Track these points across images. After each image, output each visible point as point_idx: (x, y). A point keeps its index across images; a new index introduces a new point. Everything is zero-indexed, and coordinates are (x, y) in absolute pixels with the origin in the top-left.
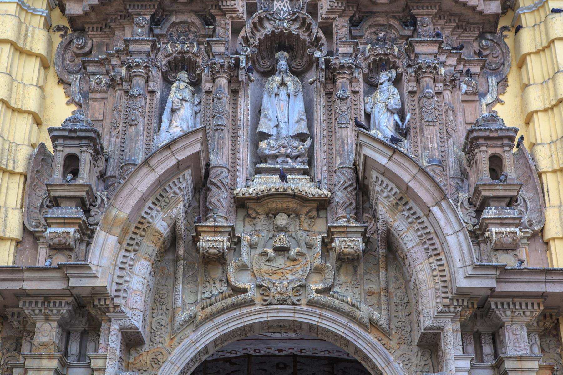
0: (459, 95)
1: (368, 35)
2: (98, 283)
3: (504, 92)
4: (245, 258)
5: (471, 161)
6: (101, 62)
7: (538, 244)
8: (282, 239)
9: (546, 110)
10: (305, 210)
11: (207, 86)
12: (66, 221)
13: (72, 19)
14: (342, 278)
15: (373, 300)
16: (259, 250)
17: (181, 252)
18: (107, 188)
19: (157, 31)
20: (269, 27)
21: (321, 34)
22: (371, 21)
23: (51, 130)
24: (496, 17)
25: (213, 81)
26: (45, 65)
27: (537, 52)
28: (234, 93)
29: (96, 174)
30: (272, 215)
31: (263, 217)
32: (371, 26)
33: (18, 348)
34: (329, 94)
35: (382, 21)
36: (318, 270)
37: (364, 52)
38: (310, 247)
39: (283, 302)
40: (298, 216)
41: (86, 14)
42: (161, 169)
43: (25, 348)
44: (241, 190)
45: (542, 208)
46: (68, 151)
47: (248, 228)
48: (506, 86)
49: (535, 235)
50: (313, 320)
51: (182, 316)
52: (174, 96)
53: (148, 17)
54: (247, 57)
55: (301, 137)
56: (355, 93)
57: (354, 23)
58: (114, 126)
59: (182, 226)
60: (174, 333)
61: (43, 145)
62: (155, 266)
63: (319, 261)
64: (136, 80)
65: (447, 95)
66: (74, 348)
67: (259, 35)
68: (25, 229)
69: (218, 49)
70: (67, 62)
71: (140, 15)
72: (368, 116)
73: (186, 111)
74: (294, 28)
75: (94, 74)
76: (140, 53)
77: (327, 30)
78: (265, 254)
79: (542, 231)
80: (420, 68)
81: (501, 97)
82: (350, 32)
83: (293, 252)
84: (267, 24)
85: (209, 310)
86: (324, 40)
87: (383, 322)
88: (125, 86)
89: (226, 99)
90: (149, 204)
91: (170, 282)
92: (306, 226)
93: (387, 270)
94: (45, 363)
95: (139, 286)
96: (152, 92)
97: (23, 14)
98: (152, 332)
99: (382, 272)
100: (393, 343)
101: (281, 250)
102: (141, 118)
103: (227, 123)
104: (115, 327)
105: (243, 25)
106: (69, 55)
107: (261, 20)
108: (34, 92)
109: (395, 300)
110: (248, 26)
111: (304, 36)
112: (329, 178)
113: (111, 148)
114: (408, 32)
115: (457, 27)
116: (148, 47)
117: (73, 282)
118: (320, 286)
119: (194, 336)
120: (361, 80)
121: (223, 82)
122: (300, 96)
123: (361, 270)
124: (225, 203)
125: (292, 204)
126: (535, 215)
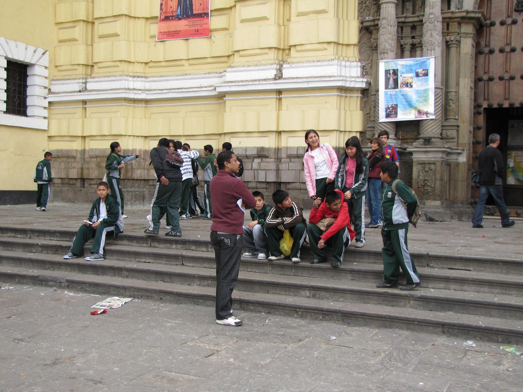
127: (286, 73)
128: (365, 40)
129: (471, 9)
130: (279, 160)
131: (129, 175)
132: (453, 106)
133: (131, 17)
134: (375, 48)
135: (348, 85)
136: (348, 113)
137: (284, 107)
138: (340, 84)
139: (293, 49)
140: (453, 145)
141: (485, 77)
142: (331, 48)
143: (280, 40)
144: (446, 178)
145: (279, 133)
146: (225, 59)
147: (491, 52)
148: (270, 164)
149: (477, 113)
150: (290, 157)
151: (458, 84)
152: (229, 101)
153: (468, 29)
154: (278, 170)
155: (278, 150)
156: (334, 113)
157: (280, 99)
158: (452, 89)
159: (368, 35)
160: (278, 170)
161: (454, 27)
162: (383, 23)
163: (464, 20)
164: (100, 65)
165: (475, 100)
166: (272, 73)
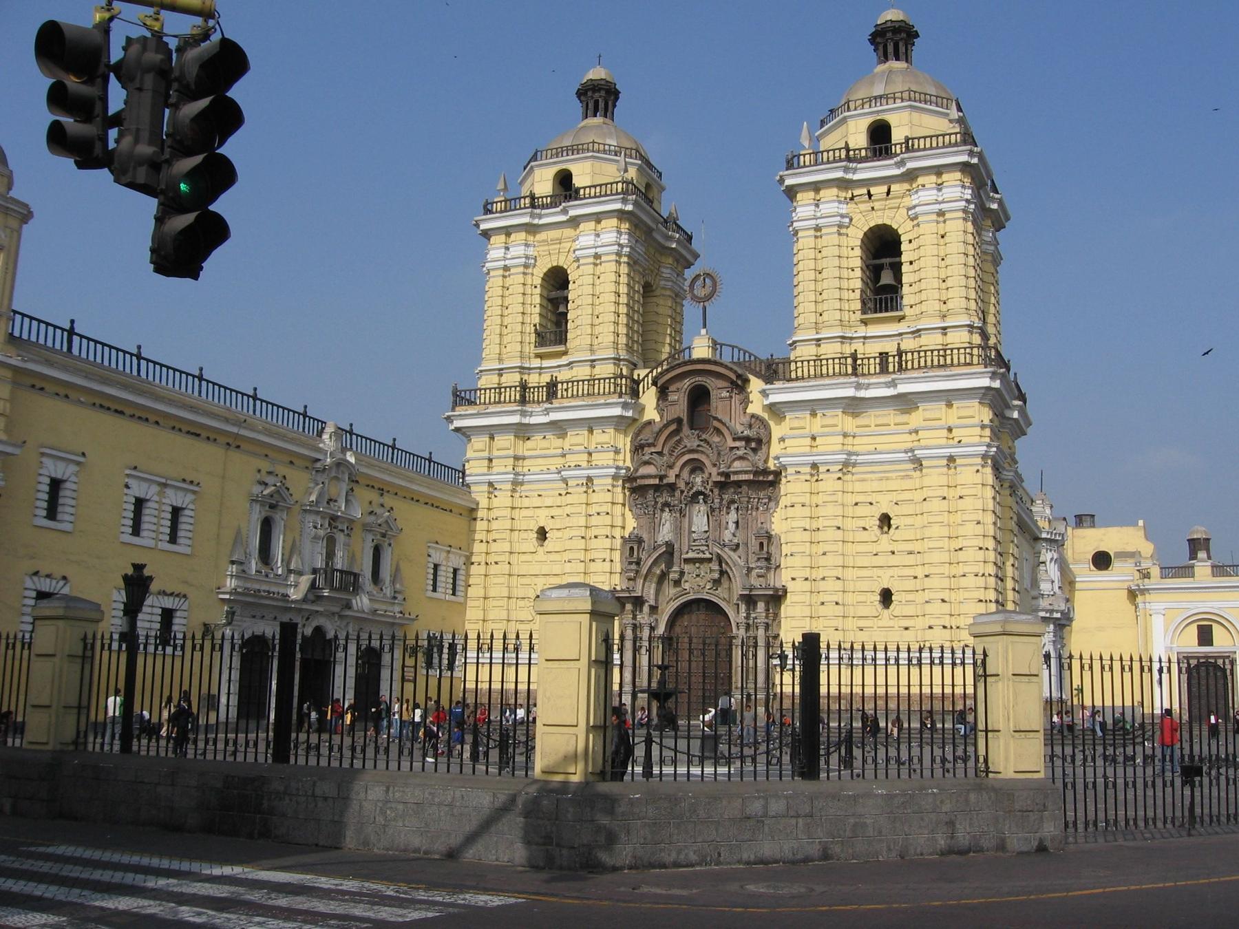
2: (640, 595)
7: (778, 570)
12: (632, 570)
20: (695, 489)
26: (624, 505)
42: (654, 557)
50: (708, 598)
52: (663, 521)
54: (686, 505)
55: (706, 532)
67: (691, 493)
68: (622, 569)
73: (668, 525)
77: (712, 491)
79: (780, 566)
101: (698, 576)
104: (647, 604)
106: (631, 499)
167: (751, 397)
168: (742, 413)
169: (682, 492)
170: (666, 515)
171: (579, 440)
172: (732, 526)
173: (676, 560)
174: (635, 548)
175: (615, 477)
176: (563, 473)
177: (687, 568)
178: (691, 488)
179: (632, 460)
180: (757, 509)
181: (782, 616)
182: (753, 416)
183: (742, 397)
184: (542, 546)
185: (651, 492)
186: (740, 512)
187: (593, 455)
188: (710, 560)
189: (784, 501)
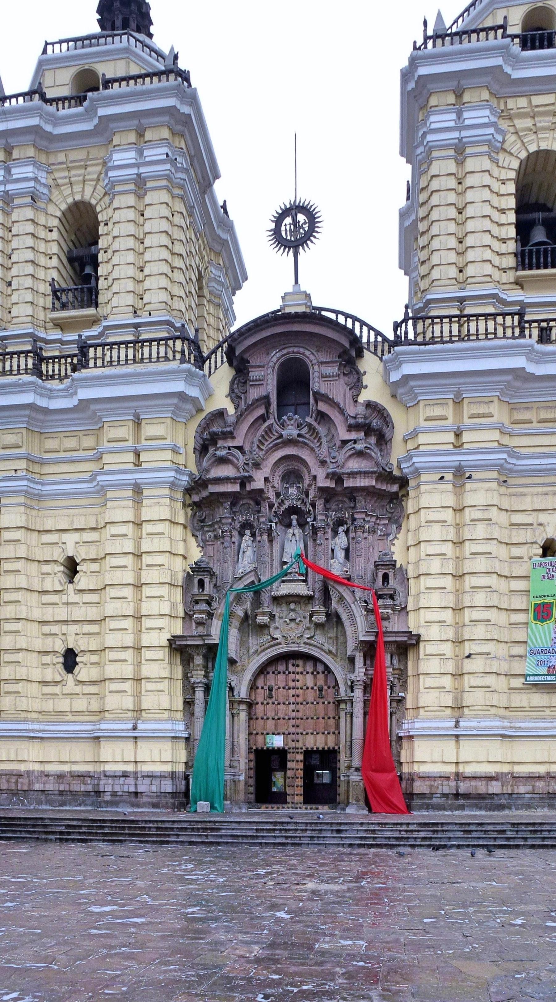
0: (376, 537)
1: (334, 507)
3: (399, 533)
4: (277, 624)
5: (377, 574)
6: (210, 526)
7: (403, 613)
8: (292, 615)
9: (414, 545)
10: (302, 601)
11: (258, 538)
12: (201, 612)
13: (195, 503)
14: (318, 632)
15: (331, 641)
16: (283, 620)
17: (250, 622)
18: (218, 591)
19: (234, 510)
20: (287, 504)
21: (311, 508)
22: (336, 499)
23: (191, 568)
24: (396, 493)
25: (261, 536)
27: (414, 513)
28: (271, 541)
29: (212, 585)
30: (288, 603)
31: (284, 605)
32: (335, 502)
33: (189, 664)
34: (315, 540)
35: (341, 498)
36: (308, 628)
37: (331, 517)
38: (305, 618)
39: (294, 643)
40: (300, 603)
41: (201, 501)
43: (191, 665)
44: (275, 593)
45: (408, 594)
46: (199, 577)
47: (279, 609)
48: (401, 529)
49: (403, 609)
51: (251, 651)
52: (243, 545)
53: (229, 503)
54: (276, 523)
56: (327, 539)
57: (327, 501)
58: (218, 560)
59: (249, 612)
60: (249, 657)
61: (188, 572)
62: (239, 630)
63: (308, 625)
64: (226, 538)
65: (370, 538)
66: (210, 665)
67: (282, 509)
68: (186, 613)
69: (262, 520)
70: (195, 524)
71: (225, 502)
72: (333, 550)
73: (249, 552)
74: (299, 504)
75: (208, 531)
76: (226, 524)
78: (286, 622)
80: (356, 527)
81: (397, 536)
82: (325, 506)
83: (297, 621)
84: (286, 502)
85: (263, 647)
86: (312, 512)
87: (334, 651)
88: (222, 540)
89: (267, 544)
90: (234, 604)
91: (246, 635)
92: (303, 608)
93: (337, 628)
94: (199, 672)
95: (233, 640)
96: (234, 543)
97: (173, 502)
98: (241, 657)
99: (335, 629)
100: (338, 660)
102: (229, 559)
103: (267, 559)
105: (274, 505)
107: (282, 501)
108: (182, 544)
109: (340, 641)
110: (276, 506)
111: (303, 508)
112: (314, 585)
113: (218, 572)
114: (352, 505)
115: (378, 498)
116: (230, 520)
117: (206, 642)
118: (308, 636)
119: (257, 658)
120: (330, 530)
121: (265, 537)
122: (302, 541)
123: (326, 629)
124: (267, 599)
125: (296, 599)
126: (404, 599)
127: (140, 726)
128: (186, 708)
129: (244, 697)
130: (136, 778)
131: (31, 787)
132: (236, 749)
133: (28, 681)
134: (193, 714)
135: (177, 735)
136: (178, 752)
137: (139, 747)
138: (173, 735)
139: (143, 712)
140: (236, 771)
141: (254, 732)
142: (166, 715)
143: (134, 705)
144: (233, 788)
145: (136, 762)
146: (98, 714)
147: (257, 719)
148: (131, 781)
149: (250, 752)
150: (143, 777)
151: (239, 737)
152: (103, 742)
153: (243, 707)
154: (136, 785)
155: (135, 773)
156: (169, 752)
157: (136, 742)
158: (236, 740)
159: (188, 706)
160: (136, 785)
161: (236, 706)
162: (197, 702)
163: (240, 702)
164: (6, 712)
165: (249, 745)
166: (130, 726)
167: (366, 380)
168: (352, 402)
169: (271, 506)
170: (247, 538)
171: (121, 432)
172: (340, 554)
173: (265, 597)
174: (207, 580)
175: (173, 486)
176: (99, 478)
177: (277, 611)
178: (282, 501)
179: (199, 463)
180: (374, 532)
181: (410, 673)
182: (369, 405)
183: (352, 379)
184: (71, 582)
185: (227, 505)
186: (352, 535)
187: (142, 454)
188: (310, 599)
189: (412, 522)
